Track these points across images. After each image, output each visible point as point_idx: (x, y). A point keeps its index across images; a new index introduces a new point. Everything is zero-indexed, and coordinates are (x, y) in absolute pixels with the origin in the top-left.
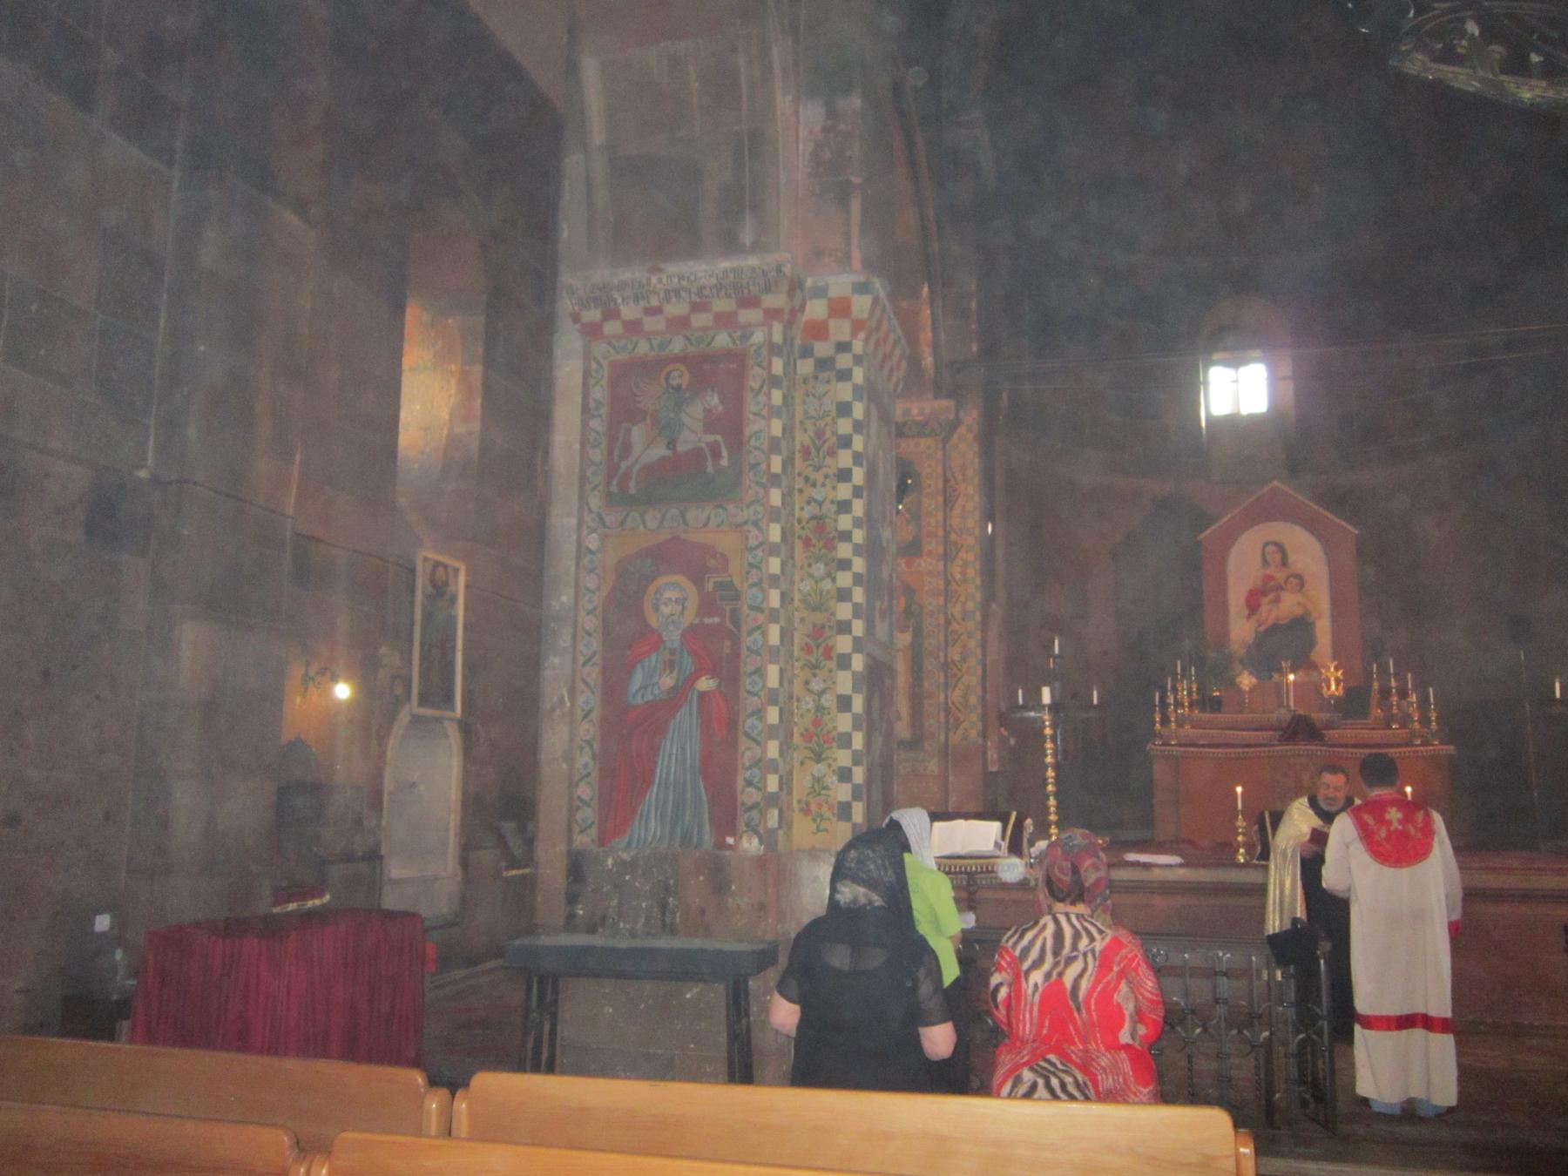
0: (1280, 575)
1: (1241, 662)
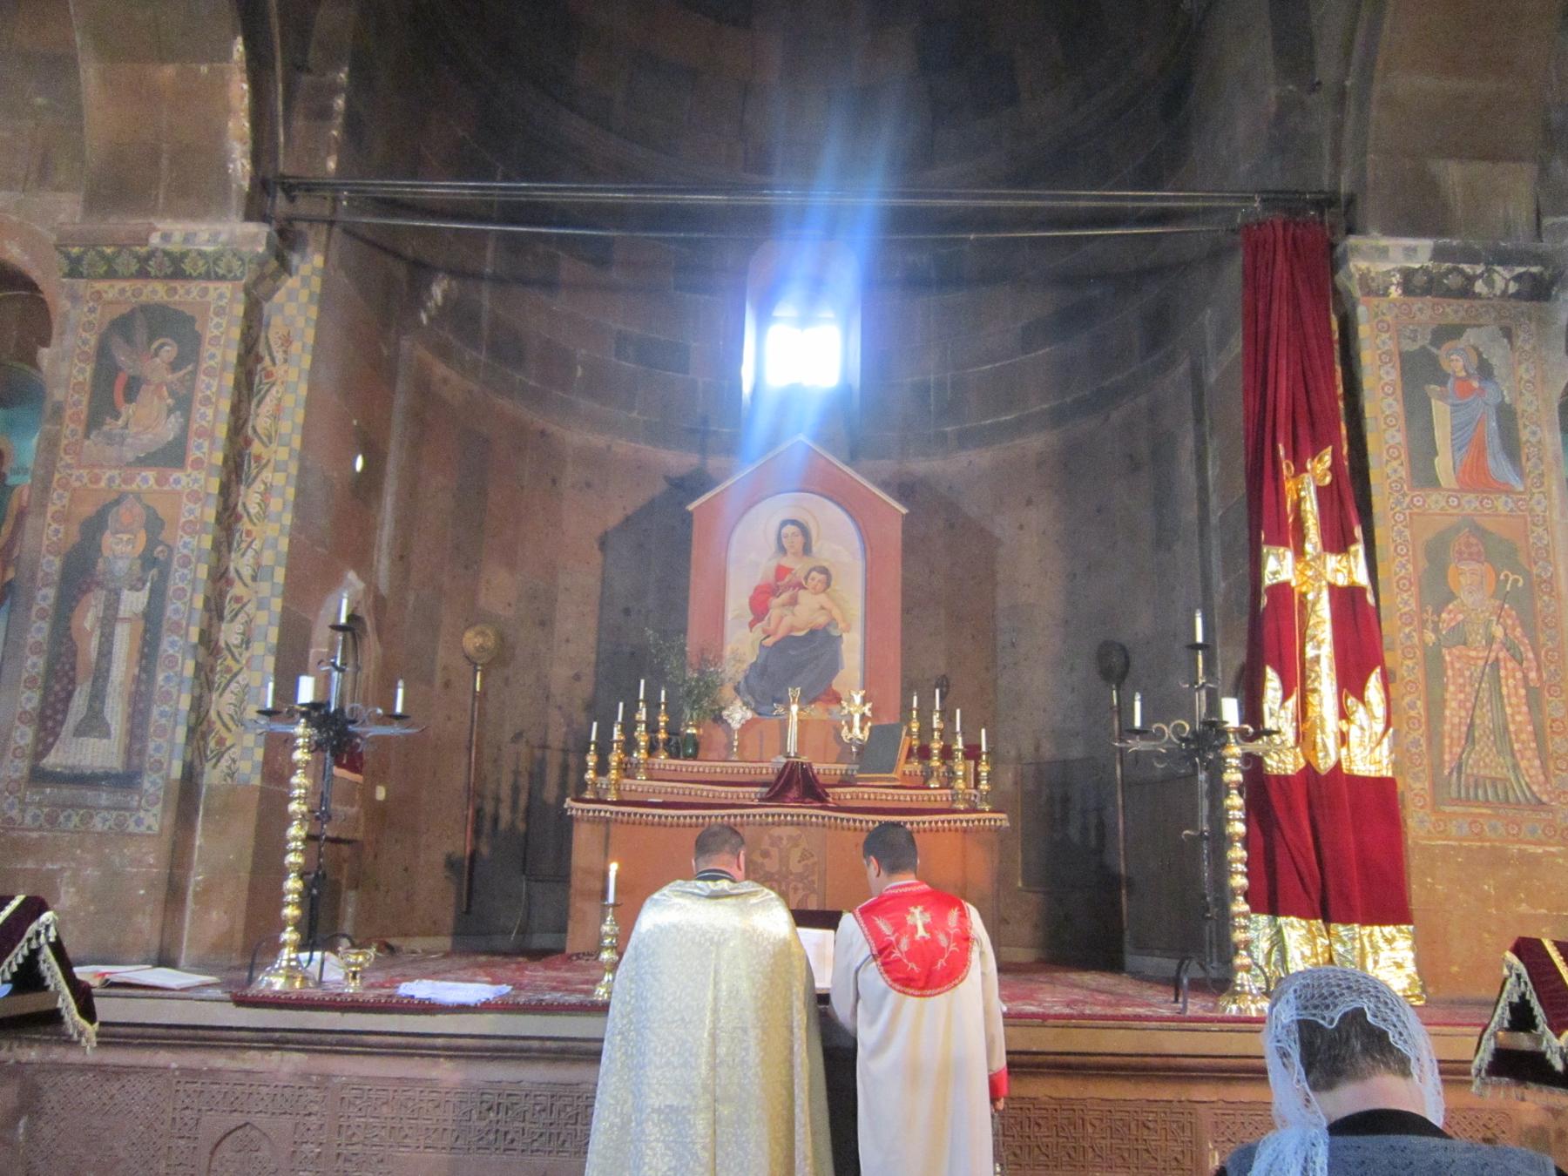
0: (799, 567)
1: (737, 689)
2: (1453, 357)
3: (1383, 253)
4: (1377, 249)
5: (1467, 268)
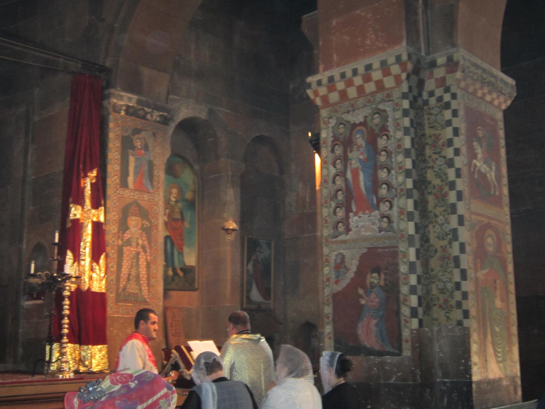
2: (138, 141)
3: (121, 98)
4: (119, 95)
5: (146, 109)
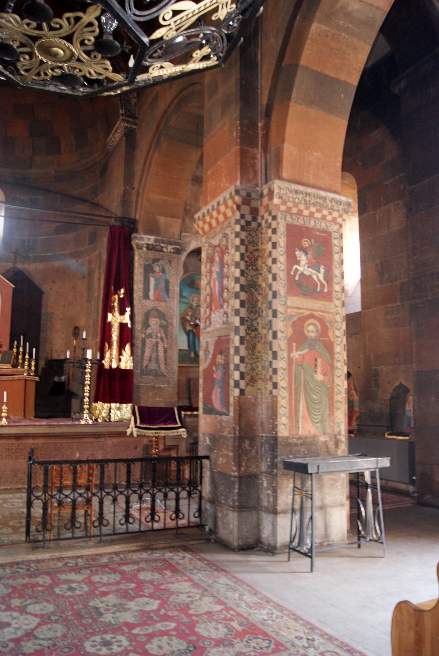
3: (142, 239)
5: (162, 245)
